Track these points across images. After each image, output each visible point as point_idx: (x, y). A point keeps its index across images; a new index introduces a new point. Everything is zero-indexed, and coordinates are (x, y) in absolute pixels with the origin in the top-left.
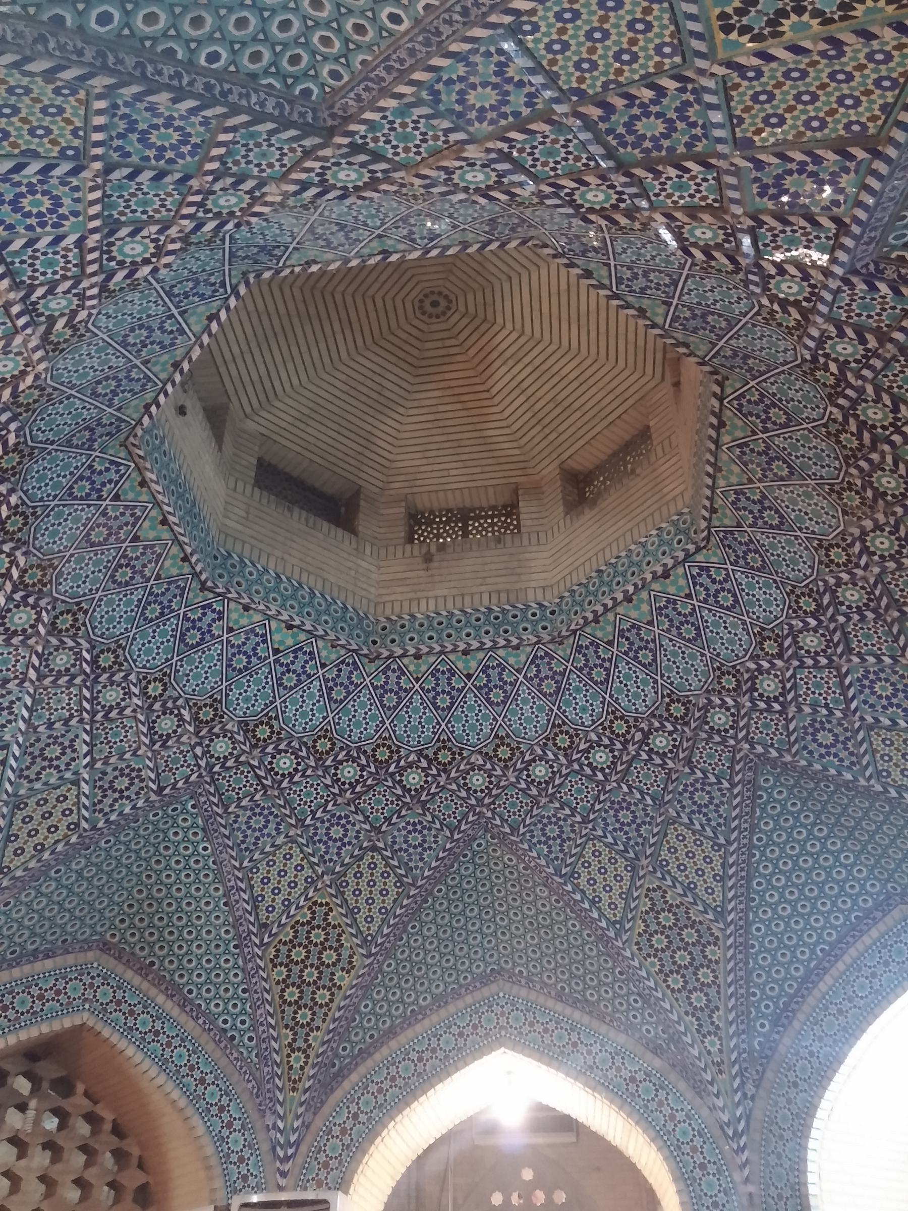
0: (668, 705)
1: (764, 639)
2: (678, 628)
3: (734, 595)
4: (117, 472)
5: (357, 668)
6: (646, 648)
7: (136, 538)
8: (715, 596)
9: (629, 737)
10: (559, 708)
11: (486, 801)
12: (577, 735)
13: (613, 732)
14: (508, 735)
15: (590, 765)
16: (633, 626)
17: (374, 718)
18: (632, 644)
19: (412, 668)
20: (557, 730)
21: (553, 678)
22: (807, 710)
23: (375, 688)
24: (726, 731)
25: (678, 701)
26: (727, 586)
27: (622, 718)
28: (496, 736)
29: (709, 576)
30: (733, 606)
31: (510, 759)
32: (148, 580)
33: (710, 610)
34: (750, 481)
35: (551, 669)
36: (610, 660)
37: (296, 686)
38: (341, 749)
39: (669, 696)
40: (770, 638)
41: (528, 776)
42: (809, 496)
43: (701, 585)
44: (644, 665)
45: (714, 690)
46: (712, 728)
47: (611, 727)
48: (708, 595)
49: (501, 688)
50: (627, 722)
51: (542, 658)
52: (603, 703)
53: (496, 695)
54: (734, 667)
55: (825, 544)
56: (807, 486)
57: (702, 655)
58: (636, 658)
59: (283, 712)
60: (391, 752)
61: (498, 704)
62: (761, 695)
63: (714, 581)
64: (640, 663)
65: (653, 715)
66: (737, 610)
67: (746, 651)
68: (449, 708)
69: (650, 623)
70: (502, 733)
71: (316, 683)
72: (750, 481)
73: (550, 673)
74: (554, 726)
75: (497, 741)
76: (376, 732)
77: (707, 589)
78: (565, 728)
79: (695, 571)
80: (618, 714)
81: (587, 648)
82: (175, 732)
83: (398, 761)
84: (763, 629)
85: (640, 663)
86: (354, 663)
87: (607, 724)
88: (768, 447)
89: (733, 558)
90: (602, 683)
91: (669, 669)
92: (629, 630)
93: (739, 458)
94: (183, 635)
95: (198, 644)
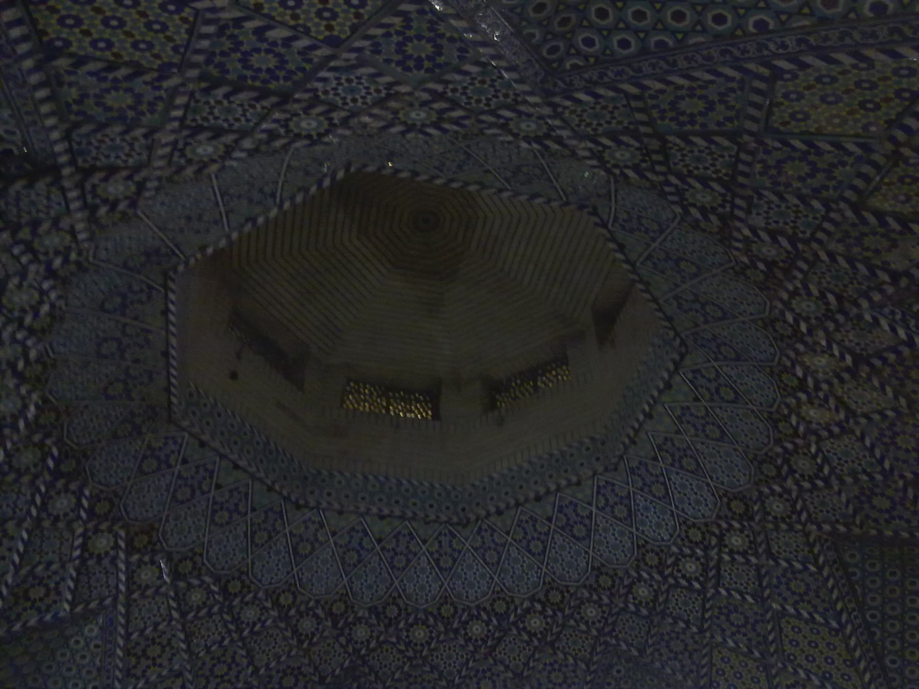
0: (728, 504)
5: (454, 536)
7: (218, 487)
10: (637, 529)
11: (607, 630)
13: (691, 541)
14: (603, 565)
15: (684, 577)
16: (666, 439)
17: (483, 576)
19: (499, 524)
22: (849, 480)
23: (476, 549)
24: (790, 517)
26: (722, 381)
29: (704, 377)
31: (613, 586)
32: (246, 514)
35: (617, 495)
37: (407, 565)
38: (464, 611)
39: (725, 495)
41: (634, 598)
45: (761, 480)
46: (775, 518)
50: (699, 529)
51: (605, 487)
52: (672, 515)
53: (579, 530)
57: (735, 450)
58: (682, 467)
59: (404, 590)
60: (507, 603)
61: (584, 539)
62: (802, 476)
63: (709, 380)
65: (719, 517)
67: (768, 437)
68: (544, 551)
69: (678, 432)
70: (596, 564)
71: (424, 558)
72: (677, 286)
75: (595, 572)
76: (489, 588)
78: (649, 547)
79: (690, 376)
81: (638, 468)
82: (317, 629)
83: (516, 609)
86: (450, 532)
94: (295, 549)
95: (311, 553)
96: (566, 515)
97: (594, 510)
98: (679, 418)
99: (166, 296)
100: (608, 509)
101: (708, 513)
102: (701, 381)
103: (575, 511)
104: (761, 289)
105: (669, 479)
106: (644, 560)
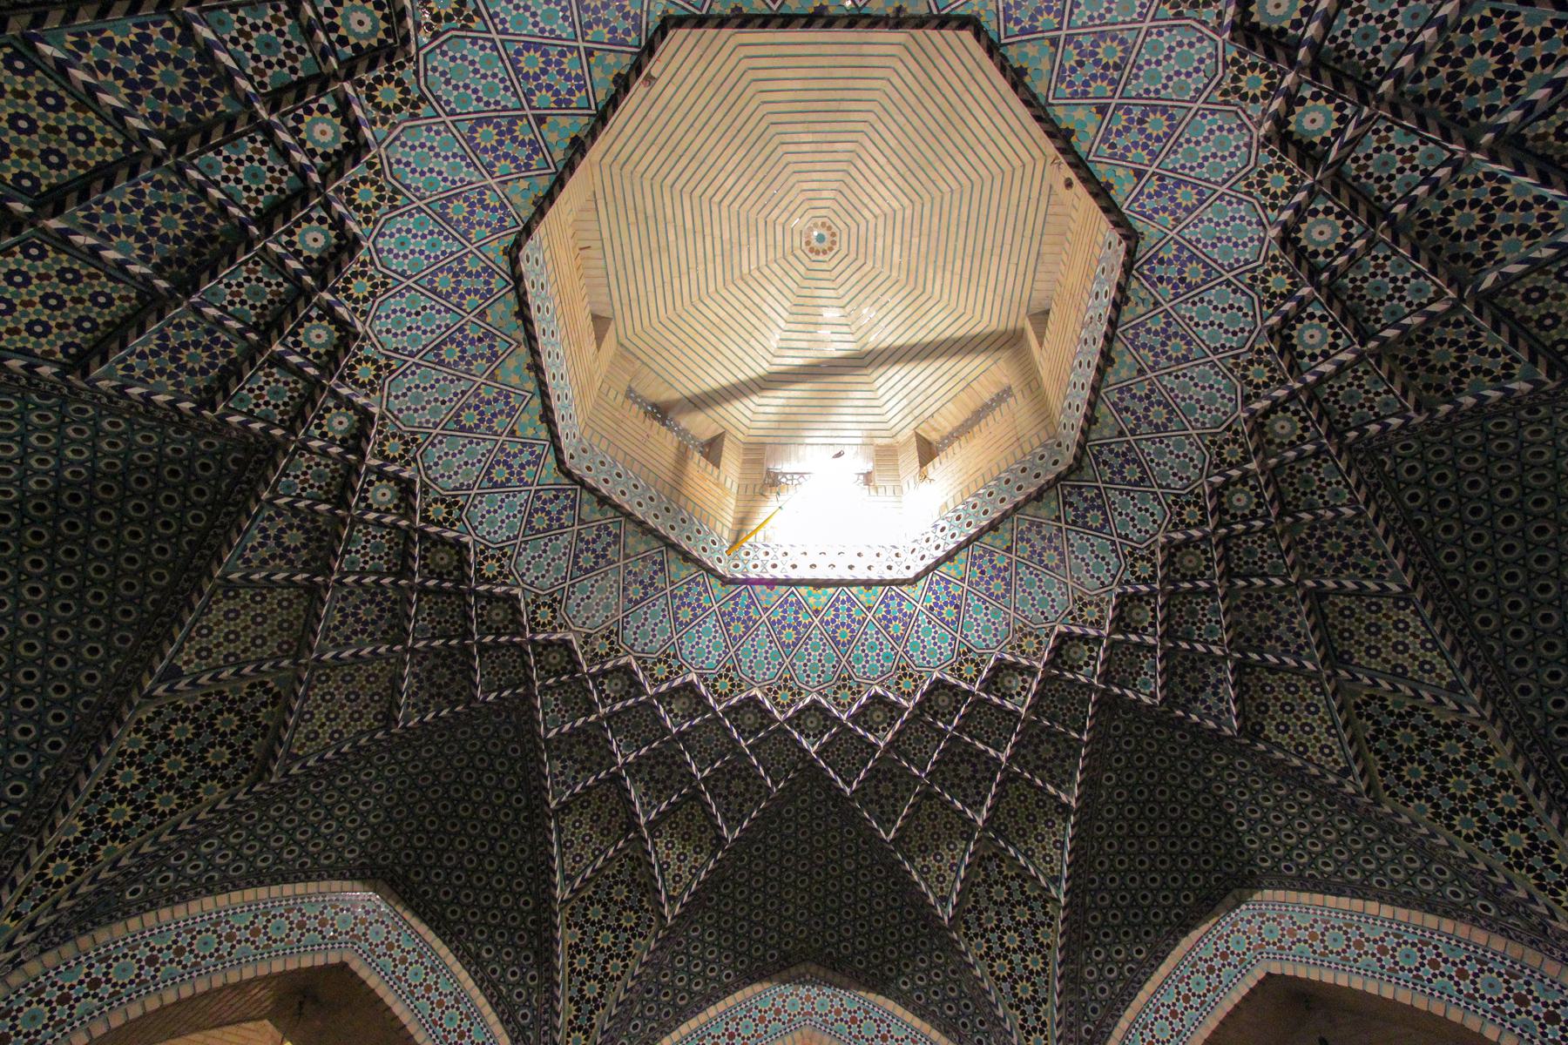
4: (1142, 206)
6: (462, 358)
9: (341, 296)
12: (367, 220)
14: (414, 116)
18: (472, 342)
20: (387, 193)
21: (466, 219)
25: (377, 377)
27: (373, 294)
28: (423, 98)
31: (370, 98)
35: (480, 223)
36: (459, 306)
39: (388, 366)
44: (438, 347)
47: (363, 274)
49: (494, 149)
50: (365, 300)
51: (501, 220)
52: (403, 274)
57: (436, 425)
61: (473, 130)
63: (522, 466)
64: (444, 343)
66: (486, 484)
70: (424, 109)
72: (627, 557)
73: (474, 219)
74: (395, 191)
75: (414, 95)
80: (380, 291)
84: (461, 508)
85: (444, 343)
87: (370, 270)
89: (544, 495)
90: (431, 282)
91: (425, 377)
96: (522, 144)
97: (490, 181)
100: (474, 197)
101: (377, 325)
102: (526, 457)
103: (515, 159)
105: (448, 310)
106: (374, 183)
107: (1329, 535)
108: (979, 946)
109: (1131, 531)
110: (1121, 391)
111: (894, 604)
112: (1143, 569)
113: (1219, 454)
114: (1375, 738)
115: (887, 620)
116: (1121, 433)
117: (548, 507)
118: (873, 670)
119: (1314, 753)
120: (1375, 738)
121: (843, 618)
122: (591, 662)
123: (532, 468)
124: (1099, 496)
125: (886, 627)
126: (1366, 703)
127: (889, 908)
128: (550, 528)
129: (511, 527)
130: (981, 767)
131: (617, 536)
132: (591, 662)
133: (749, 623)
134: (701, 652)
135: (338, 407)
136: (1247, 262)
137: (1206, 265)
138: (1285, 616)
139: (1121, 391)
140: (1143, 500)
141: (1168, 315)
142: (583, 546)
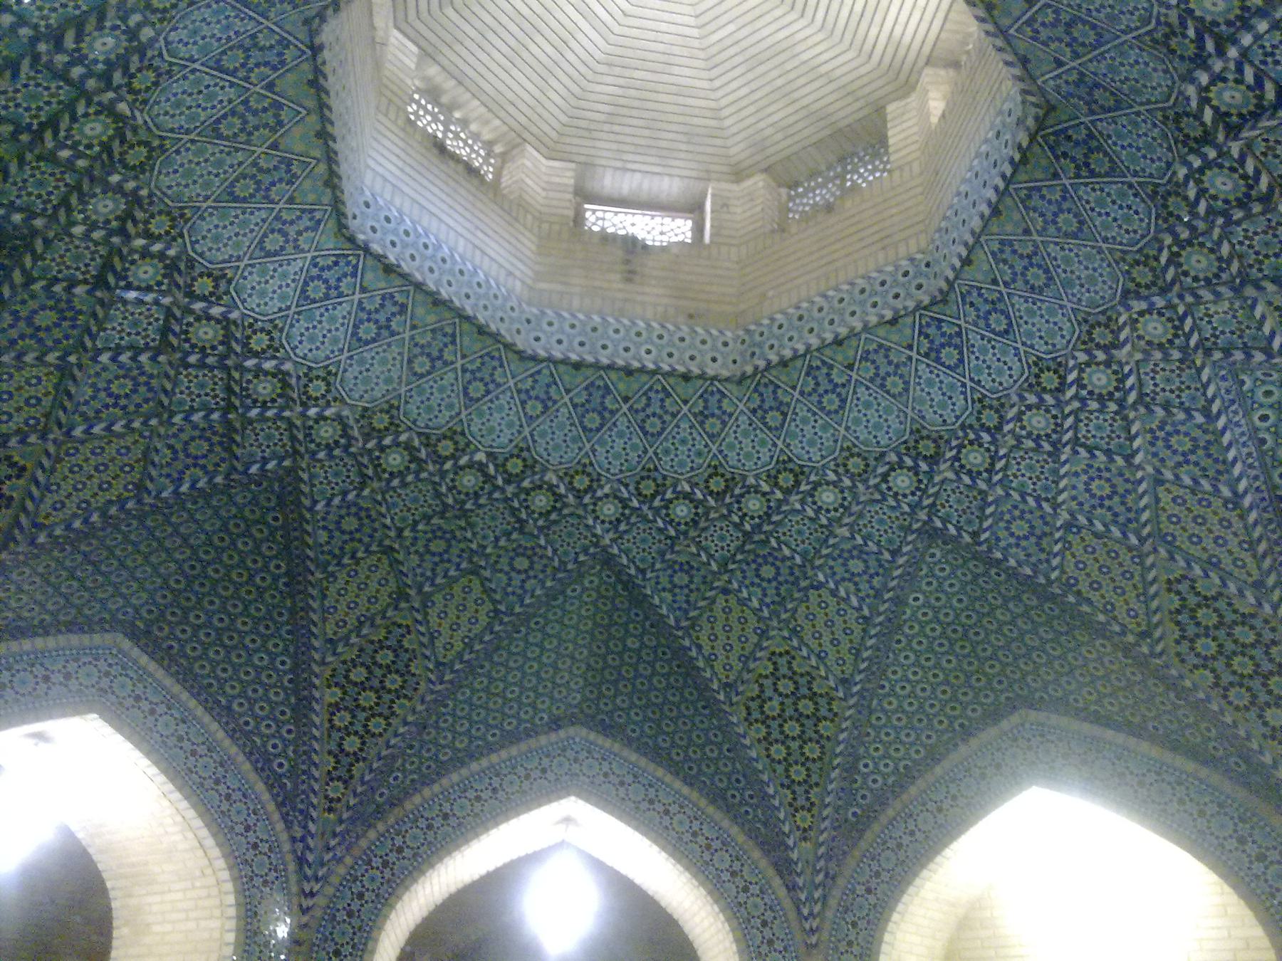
1: (216, 280)
2: (253, 177)
3: (276, 254)
8: (280, 231)
16: (280, 124)
18: (255, 113)
26: (289, 248)
29: (307, 229)
30: (262, 249)
33: (264, 221)
34: (414, 327)
40: (216, 286)
42: (388, 381)
43: (299, 218)
48: (284, 223)
54: (181, 235)
55: (331, 379)
56: (400, 383)
72: (414, 327)
77: (292, 223)
84: (229, 282)
88: (446, 363)
89: (321, 262)
91: (200, 152)
92: (276, 116)
93: (442, 329)
98: (289, 164)
99: (956, 278)
102: (306, 222)
104: (365, 409)
105: (232, 85)
107: (1178, 432)
108: (758, 731)
109: (984, 378)
110: (1002, 242)
111: (713, 401)
112: (990, 418)
113: (1089, 333)
114: (1178, 612)
115: (703, 416)
116: (995, 282)
117: (326, 274)
118: (682, 464)
119: (1121, 613)
120: (1178, 612)
121: (655, 408)
122: (367, 437)
123: (310, 234)
124: (959, 334)
125: (702, 423)
126: (1179, 581)
127: (669, 687)
128: (327, 297)
129: (283, 298)
130: (785, 571)
131: (403, 307)
132: (367, 437)
133: (547, 403)
134: (491, 430)
135: (104, 192)
136: (1151, 175)
137: (1111, 161)
138: (1121, 490)
139: (1002, 242)
140: (1005, 353)
141: (1065, 190)
142: (364, 316)
